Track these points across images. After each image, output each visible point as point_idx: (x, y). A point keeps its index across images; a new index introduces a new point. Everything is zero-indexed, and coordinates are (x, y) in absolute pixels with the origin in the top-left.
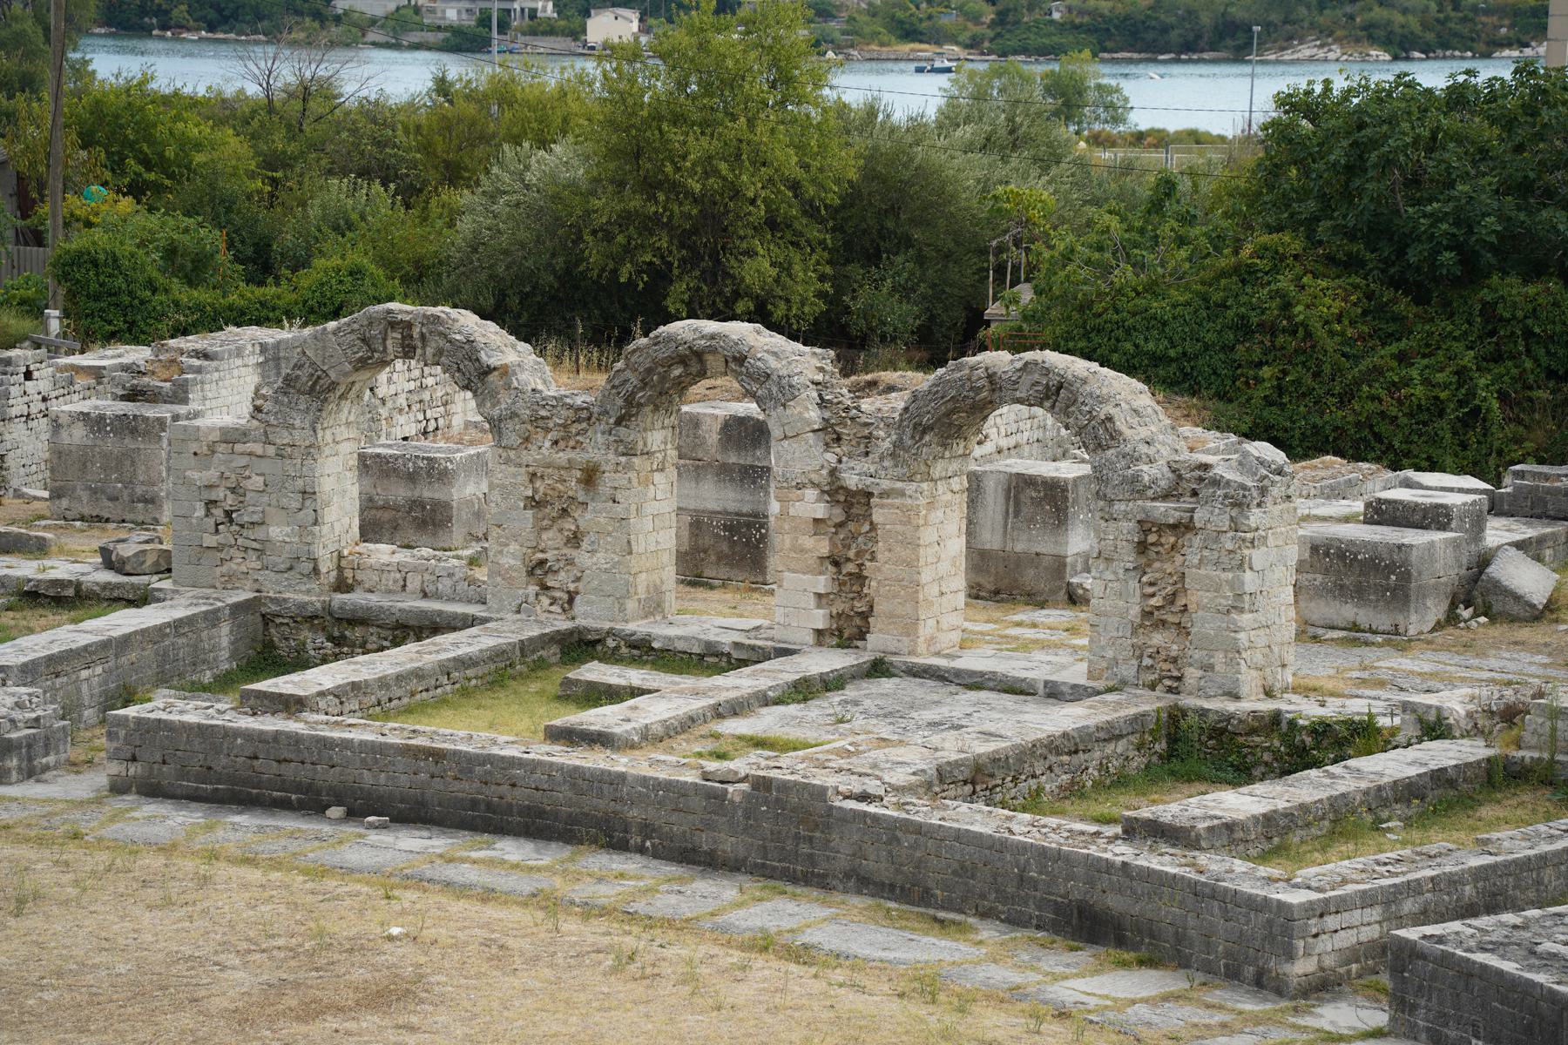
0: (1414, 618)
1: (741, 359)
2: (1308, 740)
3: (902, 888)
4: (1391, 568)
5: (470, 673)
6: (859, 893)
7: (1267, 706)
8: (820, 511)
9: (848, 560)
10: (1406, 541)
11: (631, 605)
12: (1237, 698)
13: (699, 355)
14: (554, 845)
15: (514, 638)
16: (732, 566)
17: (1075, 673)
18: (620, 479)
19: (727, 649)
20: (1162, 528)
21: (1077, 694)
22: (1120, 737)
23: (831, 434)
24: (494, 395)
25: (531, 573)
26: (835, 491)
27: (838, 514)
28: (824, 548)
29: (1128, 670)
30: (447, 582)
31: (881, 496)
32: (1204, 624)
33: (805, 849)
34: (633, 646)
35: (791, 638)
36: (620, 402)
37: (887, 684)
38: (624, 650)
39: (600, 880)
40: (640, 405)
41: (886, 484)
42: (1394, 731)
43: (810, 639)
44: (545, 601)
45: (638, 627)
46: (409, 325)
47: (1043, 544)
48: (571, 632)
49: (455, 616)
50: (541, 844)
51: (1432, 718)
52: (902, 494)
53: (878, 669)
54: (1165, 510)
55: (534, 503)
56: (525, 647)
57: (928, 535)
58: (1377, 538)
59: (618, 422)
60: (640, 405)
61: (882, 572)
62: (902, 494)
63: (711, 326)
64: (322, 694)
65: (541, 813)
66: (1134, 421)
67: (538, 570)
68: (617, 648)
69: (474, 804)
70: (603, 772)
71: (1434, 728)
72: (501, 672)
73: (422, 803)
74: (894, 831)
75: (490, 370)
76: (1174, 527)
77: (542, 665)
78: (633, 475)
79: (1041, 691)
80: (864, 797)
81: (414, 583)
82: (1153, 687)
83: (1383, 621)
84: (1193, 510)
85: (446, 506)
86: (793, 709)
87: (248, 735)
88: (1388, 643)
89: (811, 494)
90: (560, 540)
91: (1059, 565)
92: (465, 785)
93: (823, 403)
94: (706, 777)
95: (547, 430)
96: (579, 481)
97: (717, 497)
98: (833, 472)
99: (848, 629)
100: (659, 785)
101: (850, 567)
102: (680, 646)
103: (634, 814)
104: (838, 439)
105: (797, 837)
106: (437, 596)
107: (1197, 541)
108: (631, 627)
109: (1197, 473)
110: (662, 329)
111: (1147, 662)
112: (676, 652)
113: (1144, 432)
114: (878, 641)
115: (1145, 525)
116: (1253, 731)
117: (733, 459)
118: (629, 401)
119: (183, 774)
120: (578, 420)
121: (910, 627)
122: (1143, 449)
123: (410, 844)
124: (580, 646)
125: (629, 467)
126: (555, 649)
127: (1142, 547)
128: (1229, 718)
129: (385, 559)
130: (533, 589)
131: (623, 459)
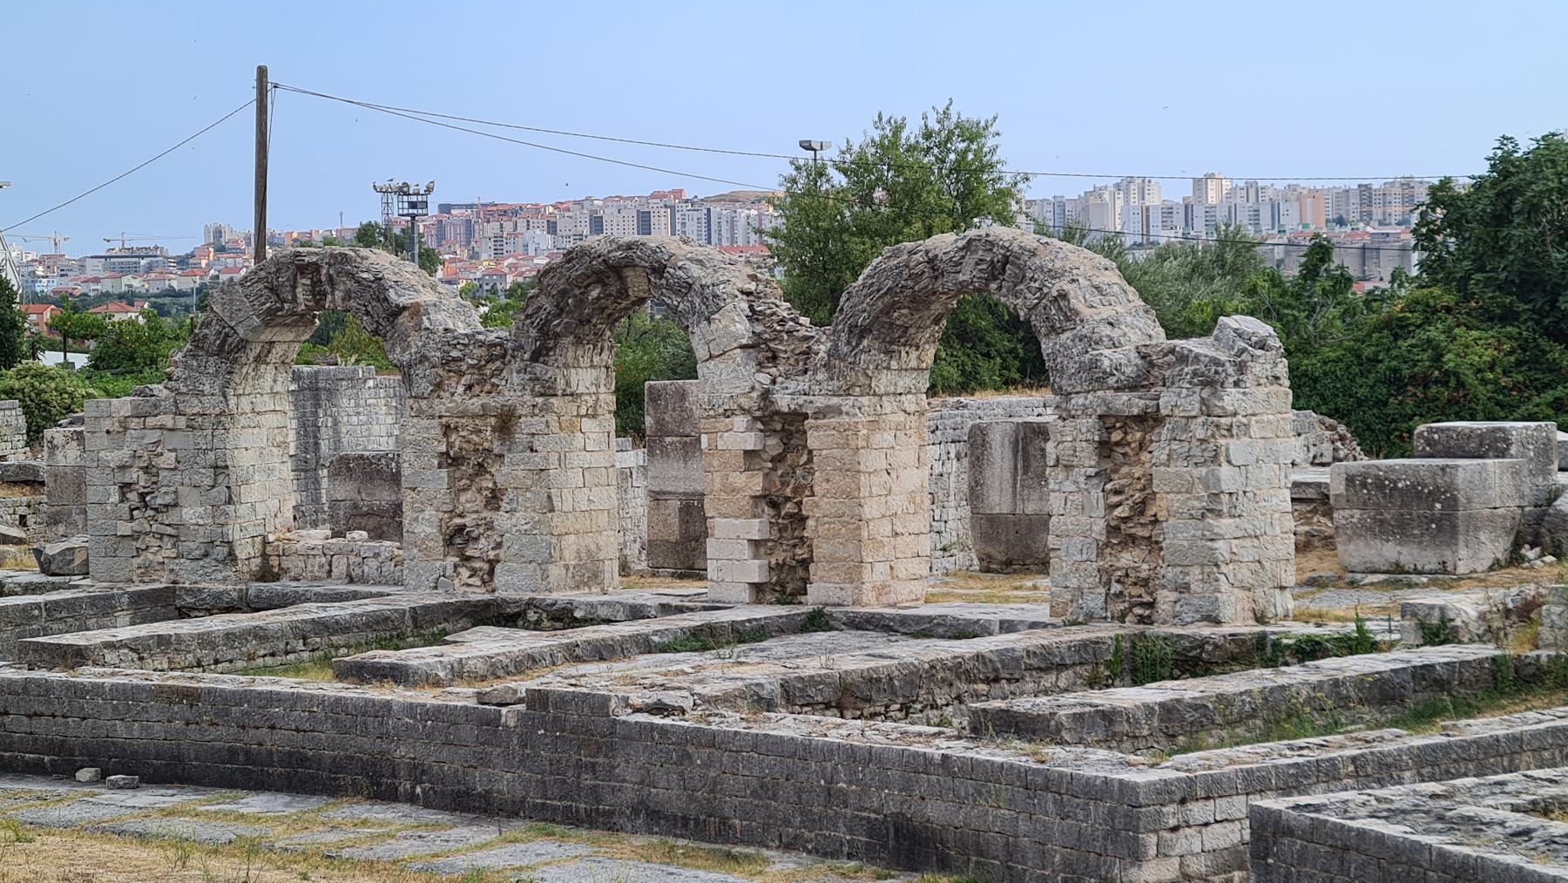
0: (1463, 552)
3: (697, 821)
4: (1435, 495)
8: (751, 441)
9: (788, 499)
11: (555, 571)
12: (1218, 622)
17: (1042, 613)
18: (537, 423)
22: (1062, 667)
23: (763, 350)
25: (449, 542)
26: (768, 417)
27: (774, 445)
28: (756, 484)
29: (1094, 601)
30: (373, 563)
32: (1177, 534)
33: (587, 780)
36: (533, 333)
38: (546, 623)
41: (820, 402)
43: (746, 595)
44: (465, 573)
45: (561, 596)
46: (316, 268)
52: (838, 411)
53: (816, 621)
55: (451, 460)
57: (872, 461)
59: (535, 357)
60: (557, 336)
61: (820, 507)
62: (838, 411)
65: (303, 760)
66: (1096, 299)
67: (456, 538)
69: (233, 753)
73: (178, 758)
78: (552, 418)
81: (340, 567)
83: (1428, 558)
88: (1434, 583)
89: (740, 421)
90: (480, 501)
92: (221, 731)
93: (754, 316)
95: (461, 374)
98: (766, 395)
99: (785, 582)
101: (789, 508)
103: (402, 752)
105: (579, 766)
107: (1165, 433)
111: (1116, 588)
113: (1106, 312)
114: (818, 593)
118: (544, 331)
120: (490, 360)
121: (853, 571)
125: (546, 409)
127: (1105, 448)
130: (453, 559)
131: (540, 400)
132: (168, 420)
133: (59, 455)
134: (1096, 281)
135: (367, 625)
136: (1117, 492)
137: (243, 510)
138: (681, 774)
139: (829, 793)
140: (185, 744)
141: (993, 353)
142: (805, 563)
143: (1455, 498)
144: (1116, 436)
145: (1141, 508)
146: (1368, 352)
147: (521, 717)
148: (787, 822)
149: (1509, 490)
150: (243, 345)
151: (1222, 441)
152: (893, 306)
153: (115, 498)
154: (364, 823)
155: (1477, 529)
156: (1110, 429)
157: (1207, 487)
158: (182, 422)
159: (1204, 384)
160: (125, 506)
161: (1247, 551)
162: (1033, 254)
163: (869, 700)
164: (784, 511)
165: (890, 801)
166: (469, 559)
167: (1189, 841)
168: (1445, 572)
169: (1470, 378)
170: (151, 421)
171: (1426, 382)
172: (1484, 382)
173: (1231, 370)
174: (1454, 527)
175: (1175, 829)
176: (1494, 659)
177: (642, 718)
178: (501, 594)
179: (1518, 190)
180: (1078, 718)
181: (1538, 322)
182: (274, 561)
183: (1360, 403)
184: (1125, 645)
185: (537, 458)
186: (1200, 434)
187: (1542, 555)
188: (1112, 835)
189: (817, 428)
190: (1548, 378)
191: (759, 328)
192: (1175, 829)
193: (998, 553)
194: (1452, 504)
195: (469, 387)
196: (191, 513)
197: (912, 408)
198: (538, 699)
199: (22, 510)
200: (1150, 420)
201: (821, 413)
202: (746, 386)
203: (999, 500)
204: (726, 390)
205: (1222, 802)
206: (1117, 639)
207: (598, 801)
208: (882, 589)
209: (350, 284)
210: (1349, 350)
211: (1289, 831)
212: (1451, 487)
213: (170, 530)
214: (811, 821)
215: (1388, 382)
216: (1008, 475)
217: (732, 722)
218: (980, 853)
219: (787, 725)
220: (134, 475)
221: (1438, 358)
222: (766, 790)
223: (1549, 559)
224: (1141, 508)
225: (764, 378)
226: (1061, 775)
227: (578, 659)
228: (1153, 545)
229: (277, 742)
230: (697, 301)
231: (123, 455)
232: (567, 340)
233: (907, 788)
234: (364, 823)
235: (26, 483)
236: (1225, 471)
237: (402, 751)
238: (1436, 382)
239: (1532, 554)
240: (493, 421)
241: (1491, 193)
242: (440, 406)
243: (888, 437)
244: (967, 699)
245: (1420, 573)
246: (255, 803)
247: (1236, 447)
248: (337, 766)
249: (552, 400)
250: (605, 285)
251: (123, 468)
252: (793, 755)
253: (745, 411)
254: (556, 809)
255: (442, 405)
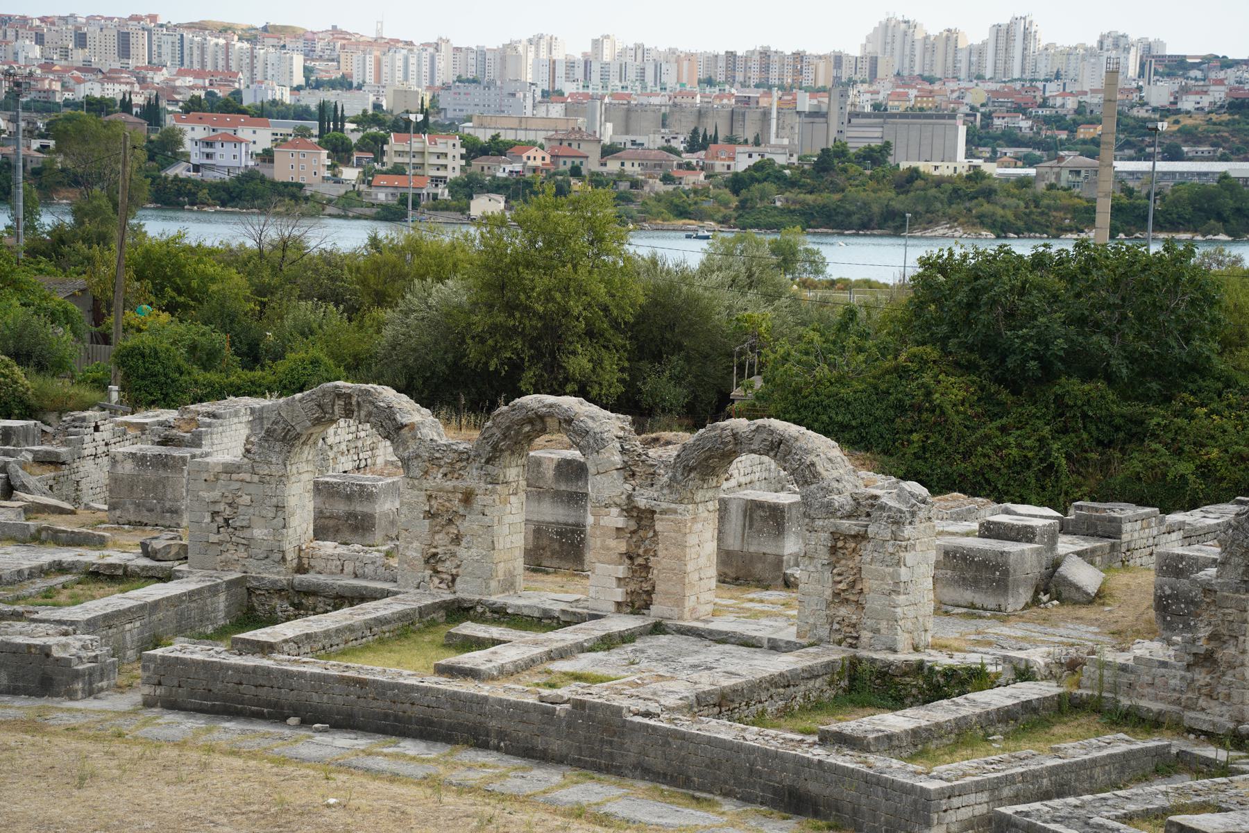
0: (1011, 600)
1: (569, 421)
2: (942, 680)
3: (672, 776)
4: (996, 567)
5: (385, 628)
6: (643, 779)
7: (914, 657)
8: (621, 522)
9: (639, 555)
10: (1006, 549)
11: (493, 584)
12: (895, 651)
13: (541, 418)
14: (439, 744)
15: (415, 605)
16: (561, 559)
17: (788, 633)
18: (488, 500)
19: (557, 614)
20: (846, 537)
21: (790, 647)
22: (817, 676)
23: (628, 471)
24: (405, 443)
25: (427, 562)
26: (630, 509)
27: (633, 525)
28: (623, 547)
29: (823, 632)
30: (371, 567)
31: (661, 513)
32: (874, 602)
33: (607, 749)
34: (493, 611)
35: (600, 607)
36: (488, 448)
37: (663, 639)
38: (488, 614)
39: (470, 768)
40: (502, 451)
41: (664, 505)
42: (998, 675)
43: (613, 608)
44: (436, 581)
45: (498, 599)
46: (350, 396)
47: (769, 548)
48: (453, 602)
49: (376, 590)
50: (430, 744)
51: (1022, 667)
52: (675, 512)
53: (658, 629)
54: (848, 526)
55: (430, 515)
56: (422, 611)
57: (692, 540)
58: (987, 547)
59: (487, 462)
60: (502, 451)
61: (661, 564)
62: (675, 512)
63: (550, 399)
64: (286, 641)
65: (431, 723)
66: (829, 466)
67: (432, 559)
68: (484, 613)
69: (386, 716)
70: (473, 695)
71: (1024, 674)
72: (405, 628)
73: (351, 715)
74: (666, 737)
75: (403, 426)
76: (855, 537)
77: (433, 623)
78: (496, 497)
79: (766, 645)
80: (647, 714)
81: (349, 568)
82: (839, 643)
83: (991, 602)
84: (867, 526)
85: (372, 516)
86: (600, 655)
87: (236, 668)
88: (994, 617)
89: (615, 511)
90: (447, 540)
91: (779, 561)
92: (380, 703)
93: (623, 451)
94: (542, 699)
95: (440, 467)
96: (460, 501)
97: (552, 513)
98: (629, 497)
99: (637, 602)
100: (510, 704)
101: (640, 561)
102: (526, 611)
103: (493, 724)
104: (633, 475)
105: (602, 741)
106: (364, 577)
107: (870, 546)
108: (493, 599)
109: (870, 501)
110: (517, 400)
111: (836, 626)
112: (523, 616)
113: (835, 474)
114: (658, 610)
115: (836, 535)
116: (905, 674)
117: (563, 487)
118: (495, 448)
119: (192, 694)
120: (461, 460)
121: (680, 601)
122: (835, 485)
123: (342, 742)
124: (459, 611)
125: (494, 492)
126: (442, 613)
127: (833, 550)
128: (891, 664)
129: (330, 551)
130: (428, 572)
131: (490, 486)
132: (247, 477)
133: (119, 467)
134: (829, 455)
135: (399, 619)
136: (839, 575)
137: (291, 531)
138: (664, 752)
139: (751, 771)
140: (356, 708)
141: (611, 346)
142: (649, 593)
143: (1007, 570)
144: (840, 544)
145: (852, 585)
146: (883, 387)
147: (568, 712)
148: (726, 782)
149: (1035, 563)
150: (298, 436)
151: (902, 554)
152: (710, 457)
153: (208, 519)
154: (484, 765)
155: (1018, 586)
156: (836, 540)
157: (892, 578)
158: (256, 478)
159: (893, 523)
160: (215, 525)
161: (911, 611)
162: (796, 439)
163: (733, 701)
164: (638, 563)
165: (788, 779)
166: (438, 572)
167: (952, 817)
168: (1000, 611)
169: (950, 411)
170: (234, 476)
171: (919, 409)
172: (958, 412)
173: (908, 515)
174: (1006, 586)
175: (945, 811)
176: (1059, 695)
177: (638, 719)
178: (460, 595)
179: (985, 289)
180: (877, 739)
181: (991, 372)
182: (305, 561)
183: (876, 420)
184: (847, 662)
185: (486, 519)
186: (891, 550)
187: (1051, 599)
188: (915, 812)
189: (662, 520)
190: (996, 409)
191: (626, 458)
192: (945, 811)
193: (731, 573)
194: (1006, 573)
195: (445, 475)
196: (258, 533)
197: (711, 508)
198: (579, 705)
199: (51, 482)
200: (861, 537)
201: (663, 512)
202: (618, 491)
203: (734, 544)
204: (606, 494)
205: (965, 797)
206: (843, 659)
207: (613, 759)
208: (693, 610)
209: (371, 408)
210: (870, 384)
211: (1015, 825)
212: (1006, 564)
213: (244, 541)
214: (739, 783)
215: (895, 407)
216: (739, 529)
217: (686, 725)
218: (838, 810)
219: (722, 730)
220: (221, 507)
221: (929, 394)
222: (713, 765)
223: (1055, 602)
224: (852, 585)
225: (628, 487)
226: (887, 779)
227: (552, 659)
228: (859, 605)
229: (417, 711)
230: (592, 441)
231: (216, 494)
232: (507, 453)
233: (797, 773)
234: (484, 765)
235: (51, 463)
236: (903, 570)
237: (493, 723)
238: (927, 410)
239: (1045, 598)
240: (460, 496)
241: (966, 289)
242: (425, 484)
243: (700, 525)
244: (775, 698)
245: (986, 610)
246: (410, 747)
247: (909, 557)
248: (452, 727)
249: (498, 487)
250: (533, 425)
251: (215, 502)
252: (731, 749)
253: (617, 505)
254: (586, 762)
255: (429, 484)
